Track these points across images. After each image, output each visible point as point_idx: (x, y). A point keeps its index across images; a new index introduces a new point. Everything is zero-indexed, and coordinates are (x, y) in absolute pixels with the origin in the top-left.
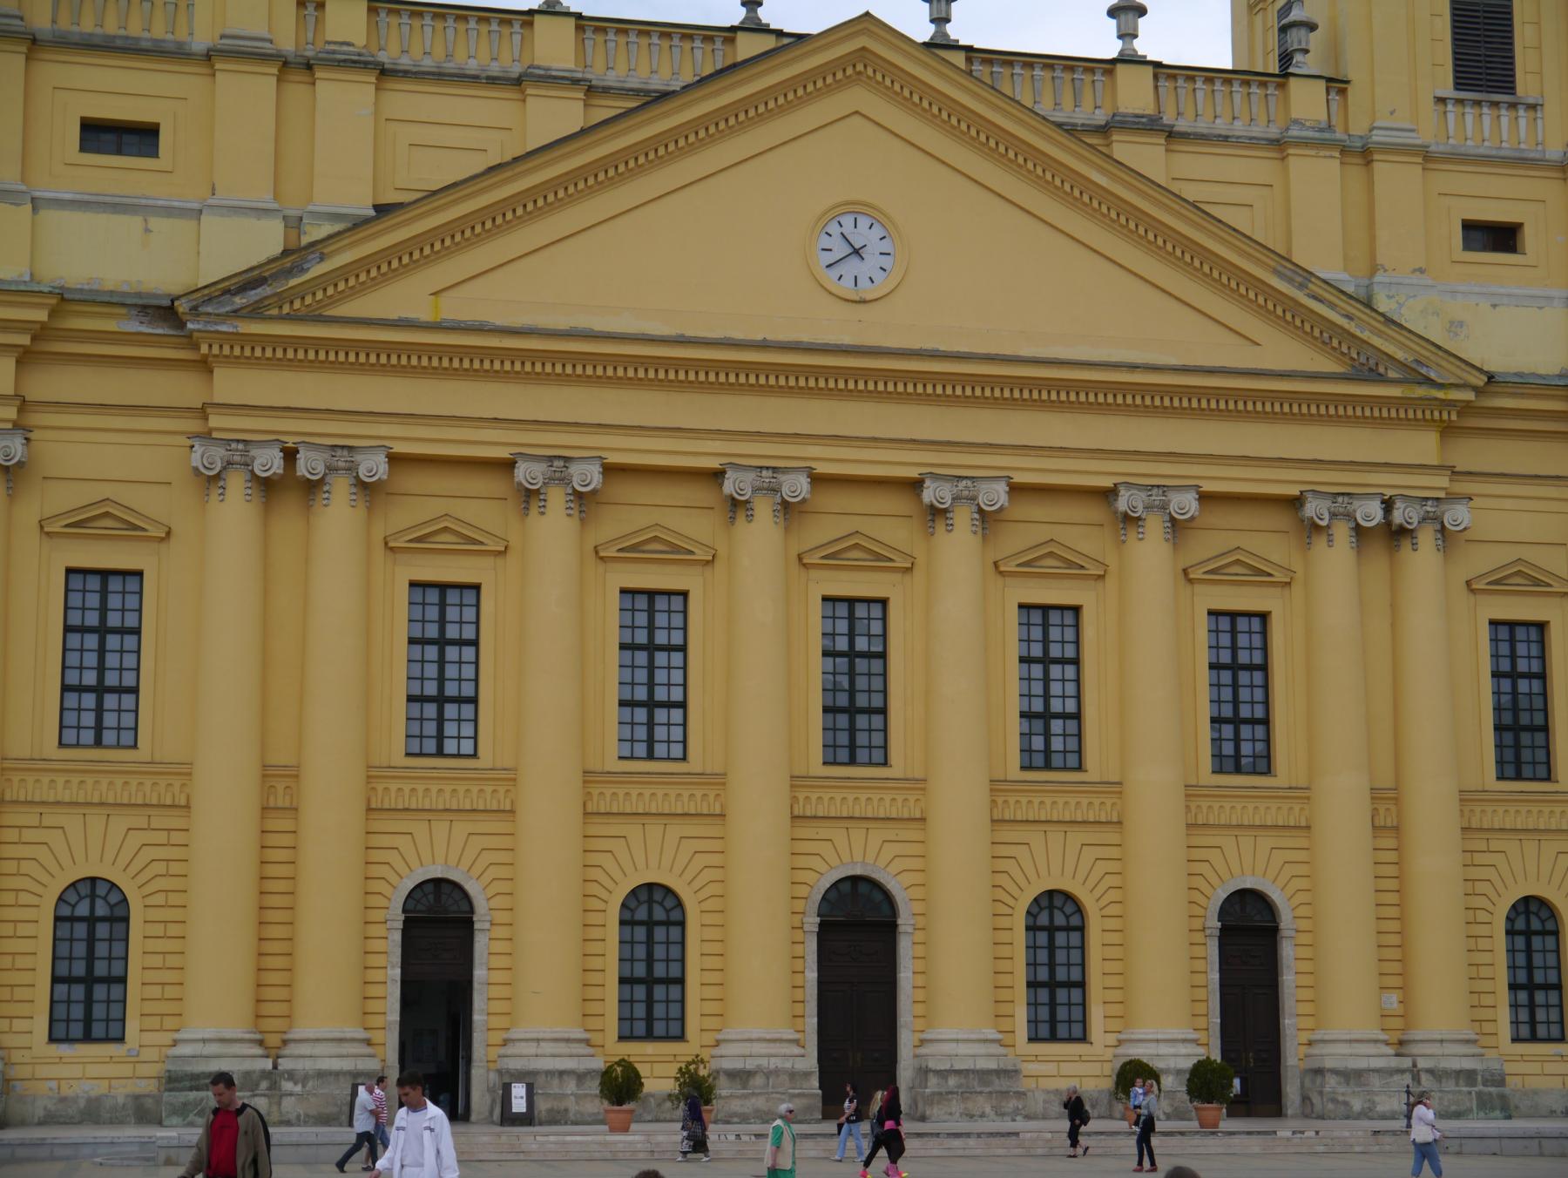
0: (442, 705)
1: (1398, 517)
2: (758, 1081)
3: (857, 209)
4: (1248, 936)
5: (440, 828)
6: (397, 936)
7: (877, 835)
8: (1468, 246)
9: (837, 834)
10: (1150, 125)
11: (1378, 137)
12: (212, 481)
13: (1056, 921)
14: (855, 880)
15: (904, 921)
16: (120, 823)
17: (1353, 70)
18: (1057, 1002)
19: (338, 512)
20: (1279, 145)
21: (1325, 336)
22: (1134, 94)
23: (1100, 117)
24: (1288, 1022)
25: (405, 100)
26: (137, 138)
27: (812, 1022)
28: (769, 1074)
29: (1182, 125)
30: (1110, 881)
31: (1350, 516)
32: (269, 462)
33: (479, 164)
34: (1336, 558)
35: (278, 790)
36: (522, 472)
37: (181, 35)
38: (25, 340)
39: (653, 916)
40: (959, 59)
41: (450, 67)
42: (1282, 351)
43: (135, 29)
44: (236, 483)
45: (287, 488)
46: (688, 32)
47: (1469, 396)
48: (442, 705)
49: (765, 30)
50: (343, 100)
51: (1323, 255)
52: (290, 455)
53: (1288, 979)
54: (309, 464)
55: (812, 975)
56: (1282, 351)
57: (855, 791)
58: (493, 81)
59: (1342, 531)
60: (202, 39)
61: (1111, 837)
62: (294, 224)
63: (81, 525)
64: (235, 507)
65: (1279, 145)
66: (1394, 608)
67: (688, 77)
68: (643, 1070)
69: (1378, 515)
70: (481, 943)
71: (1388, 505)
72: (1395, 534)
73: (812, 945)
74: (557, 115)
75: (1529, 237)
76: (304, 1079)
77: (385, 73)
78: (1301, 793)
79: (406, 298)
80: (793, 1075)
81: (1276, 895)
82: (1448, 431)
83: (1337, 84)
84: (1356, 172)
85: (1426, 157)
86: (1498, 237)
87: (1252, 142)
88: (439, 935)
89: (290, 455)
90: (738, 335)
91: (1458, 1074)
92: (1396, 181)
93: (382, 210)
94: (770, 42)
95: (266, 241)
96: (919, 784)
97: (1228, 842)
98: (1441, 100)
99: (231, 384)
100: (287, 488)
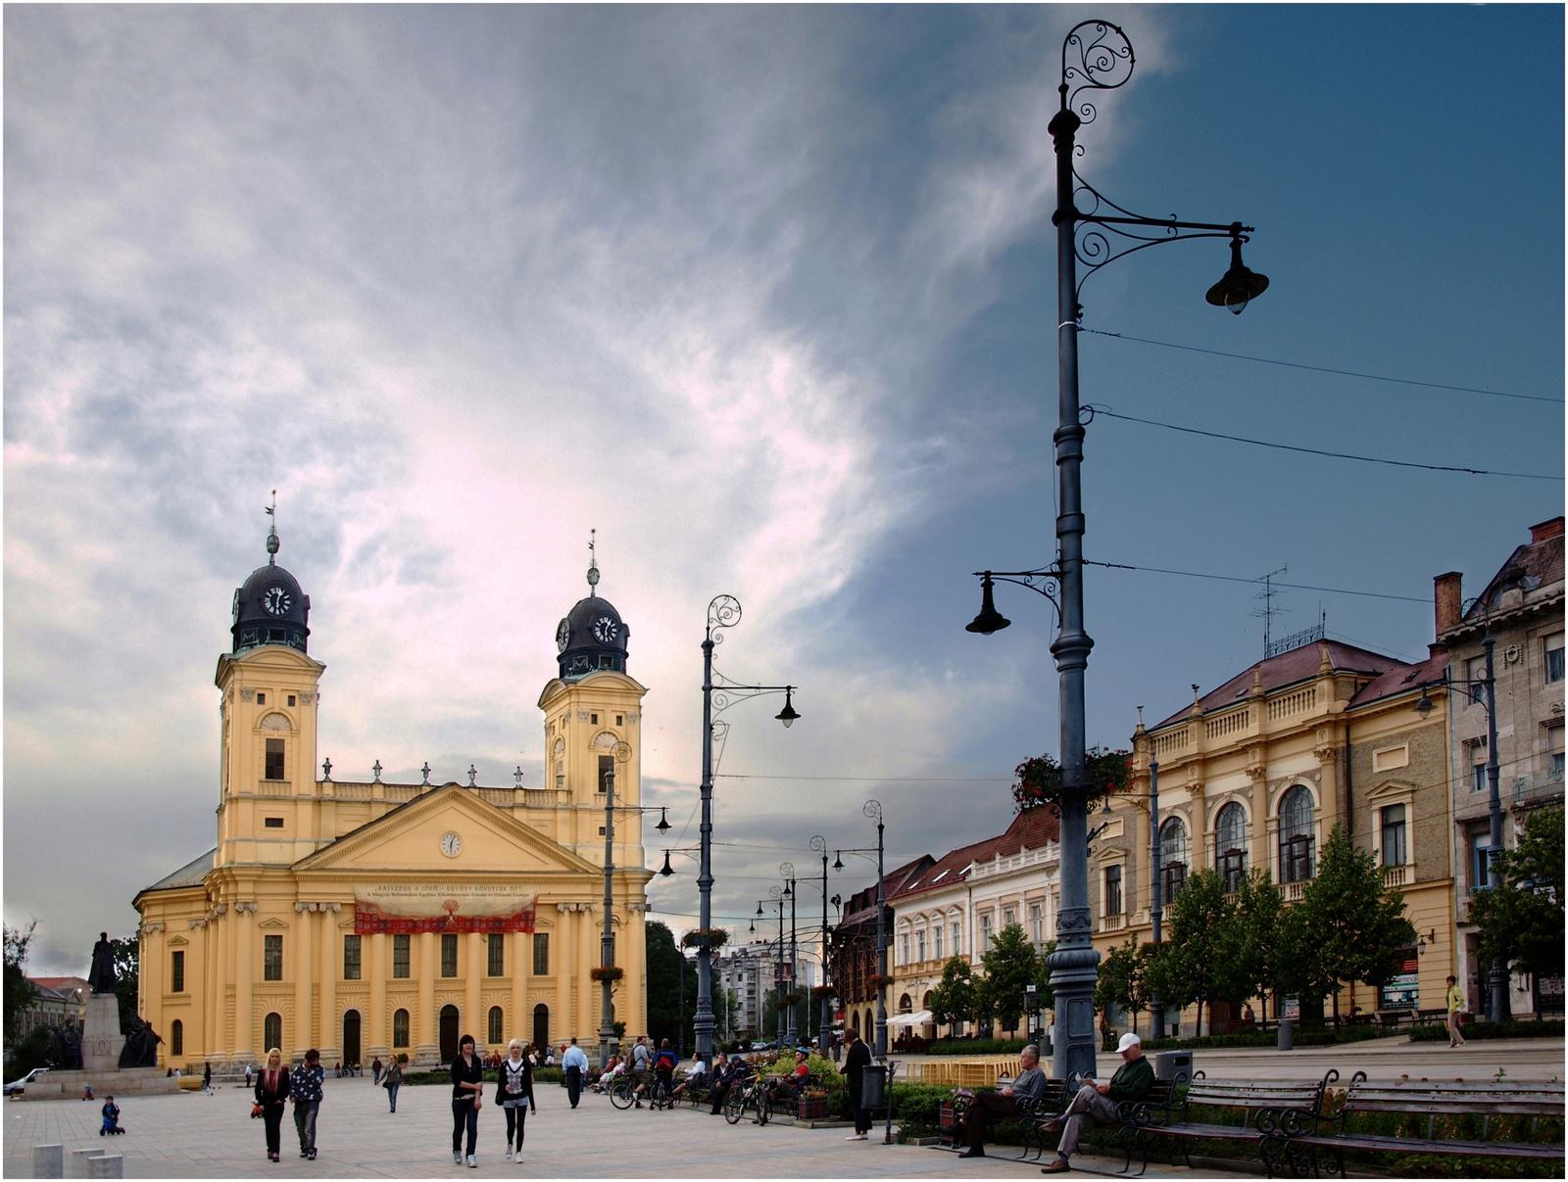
1: (580, 908)
2: (427, 1056)
4: (541, 1015)
5: (353, 997)
6: (343, 1024)
7: (455, 994)
9: (445, 994)
10: (524, 806)
11: (579, 806)
12: (299, 913)
14: (448, 1006)
15: (460, 1015)
16: (279, 999)
17: (575, 790)
19: (329, 918)
20: (555, 809)
22: (520, 797)
23: (511, 804)
24: (549, 1036)
27: (439, 1041)
28: (430, 1054)
29: (531, 805)
31: (568, 908)
32: (314, 908)
33: (359, 825)
34: (566, 918)
35: (316, 989)
37: (288, 794)
38: (256, 879)
39: (402, 1015)
40: (476, 792)
41: (353, 799)
42: (554, 866)
43: (277, 794)
44: (305, 913)
45: (318, 913)
46: (411, 787)
47: (598, 876)
49: (429, 785)
50: (328, 810)
51: (564, 840)
52: (318, 904)
53: (550, 1025)
54: (322, 908)
55: (439, 1030)
56: (554, 866)
57: (449, 983)
58: (364, 802)
59: (566, 913)
60: (294, 794)
61: (509, 992)
62: (317, 843)
63: (268, 925)
64: (305, 918)
66: (578, 930)
67: (410, 799)
68: (408, 1054)
70: (362, 1025)
71: (578, 905)
72: (579, 912)
73: (439, 1022)
76: (325, 1059)
77: (338, 802)
78: (555, 979)
79: (345, 863)
80: (435, 1054)
81: (548, 1005)
83: (570, 792)
84: (573, 815)
87: (548, 809)
88: (352, 1022)
89: (318, 904)
90: (423, 868)
91: (588, 1047)
93: (339, 839)
94: (431, 788)
95: (310, 849)
96: (464, 981)
97: (537, 992)
98: (596, 795)
99: (303, 888)
100: (318, 913)
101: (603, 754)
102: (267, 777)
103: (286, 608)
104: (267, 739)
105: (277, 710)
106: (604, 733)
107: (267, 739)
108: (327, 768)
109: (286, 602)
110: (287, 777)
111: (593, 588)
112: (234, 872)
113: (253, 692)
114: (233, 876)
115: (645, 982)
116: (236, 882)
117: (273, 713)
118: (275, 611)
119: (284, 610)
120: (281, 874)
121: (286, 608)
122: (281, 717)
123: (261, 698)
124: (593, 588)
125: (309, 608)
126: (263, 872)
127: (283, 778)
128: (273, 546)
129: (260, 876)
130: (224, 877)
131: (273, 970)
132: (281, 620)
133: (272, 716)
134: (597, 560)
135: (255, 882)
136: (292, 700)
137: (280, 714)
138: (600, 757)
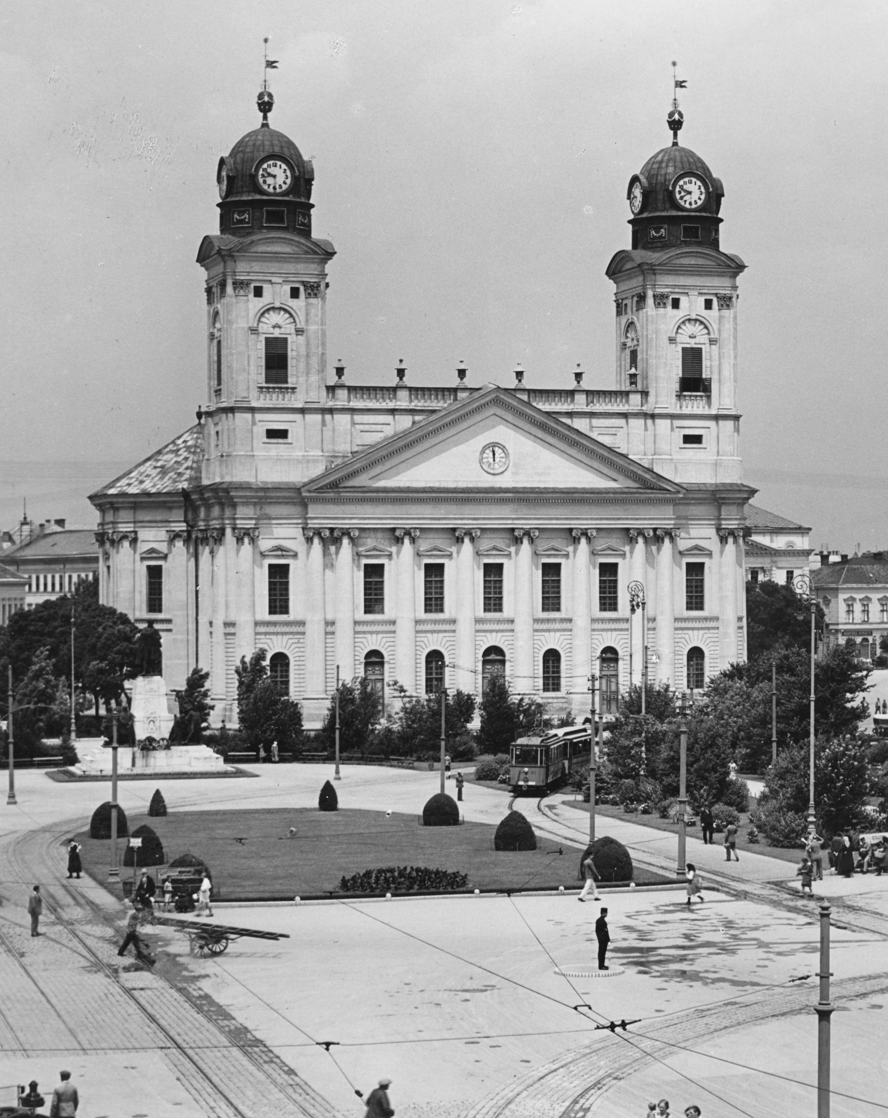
0: (374, 598)
3: (493, 446)
8: (685, 442)
11: (657, 411)
12: (309, 540)
13: (552, 658)
18: (552, 681)
20: (625, 416)
21: (636, 477)
25: (358, 418)
26: (282, 434)
30: (569, 646)
36: (397, 533)
48: (374, 598)
50: (343, 419)
65: (625, 416)
69: (651, 533)
74: (405, 422)
75: (704, 438)
82: (675, 505)
83: (645, 394)
85: (672, 417)
86: (693, 439)
92: (663, 425)
99: (314, 510)
101: (688, 346)
102: (267, 382)
104: (266, 338)
105: (277, 305)
106: (689, 320)
107: (266, 338)
108: (340, 371)
110: (291, 381)
111: (675, 135)
112: (232, 494)
113: (248, 284)
114: (232, 498)
115: (744, 622)
116: (234, 506)
120: (291, 494)
124: (675, 135)
125: (313, 179)
126: (266, 496)
127: (287, 382)
129: (260, 498)
130: (219, 498)
131: (279, 601)
134: (679, 102)
135: (255, 504)
138: (684, 349)
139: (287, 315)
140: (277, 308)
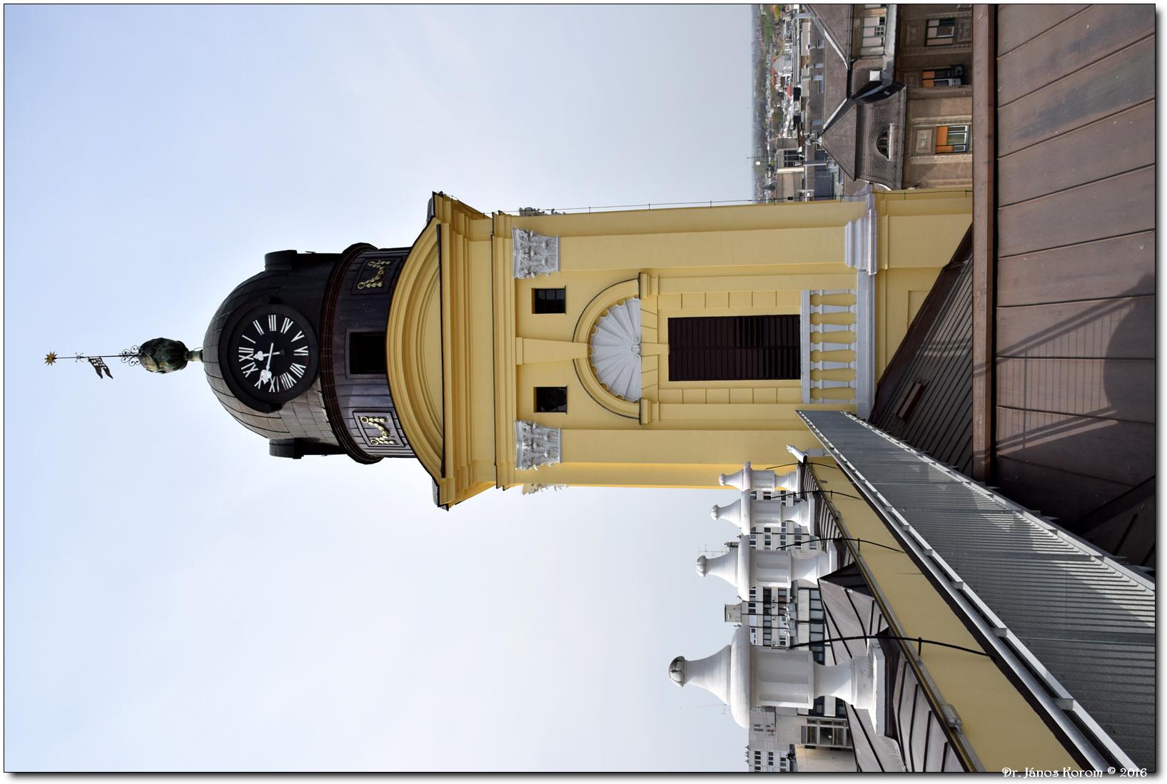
102: (796, 375)
103: (287, 325)
105: (580, 351)
109: (273, 326)
117: (590, 360)
118: (300, 360)
119: (293, 332)
121: (287, 325)
122: (600, 335)
123: (550, 399)
128: (166, 354)
132: (320, 342)
133: (600, 366)
136: (549, 302)
137: (590, 341)
139: (609, 322)
140: (590, 351)
